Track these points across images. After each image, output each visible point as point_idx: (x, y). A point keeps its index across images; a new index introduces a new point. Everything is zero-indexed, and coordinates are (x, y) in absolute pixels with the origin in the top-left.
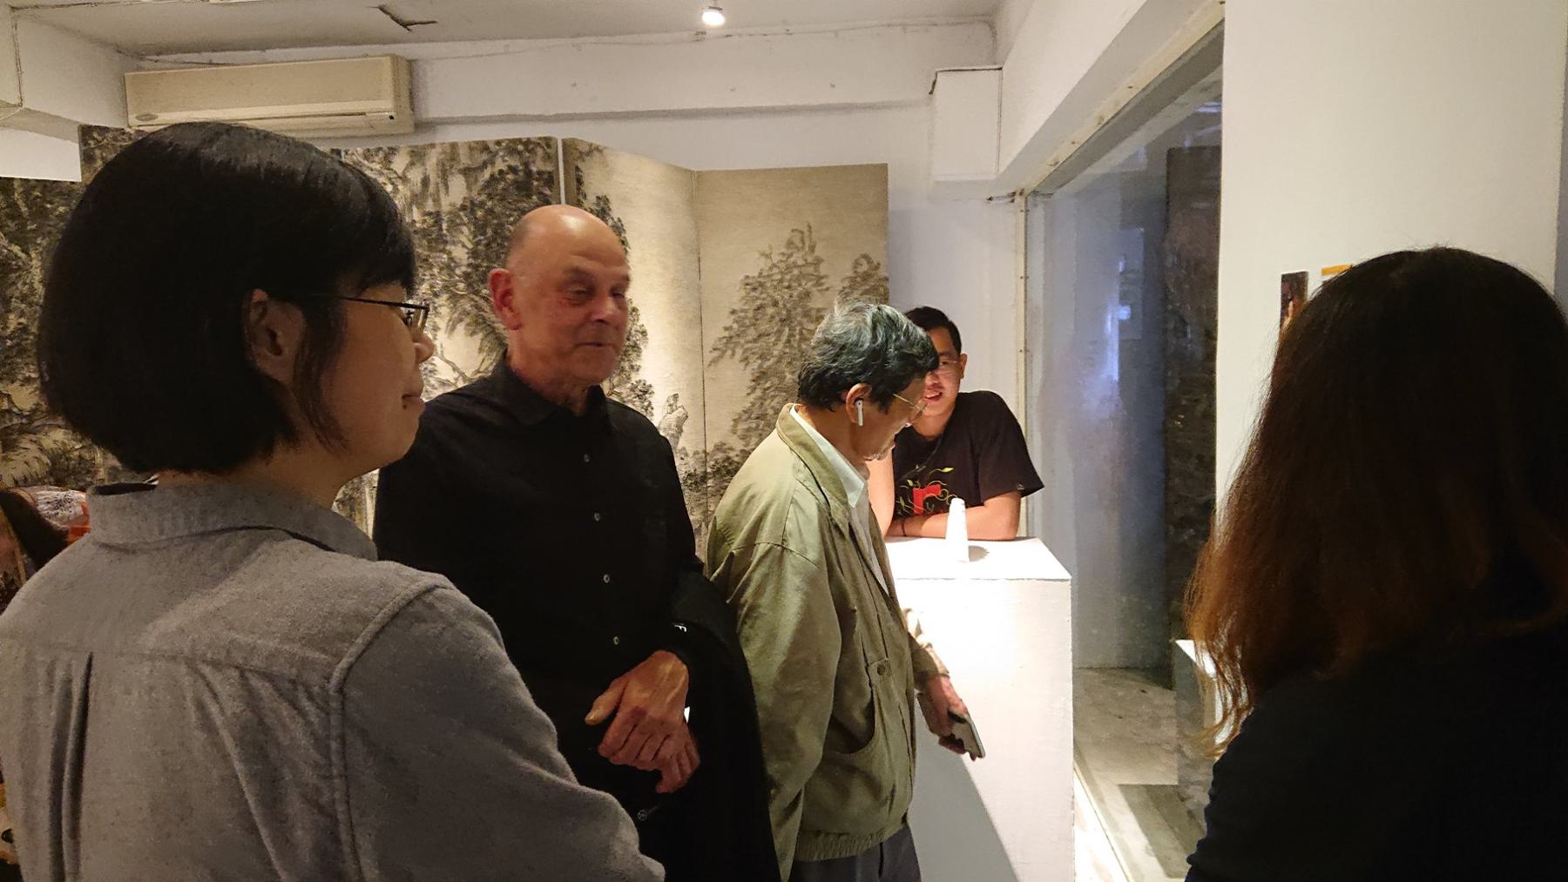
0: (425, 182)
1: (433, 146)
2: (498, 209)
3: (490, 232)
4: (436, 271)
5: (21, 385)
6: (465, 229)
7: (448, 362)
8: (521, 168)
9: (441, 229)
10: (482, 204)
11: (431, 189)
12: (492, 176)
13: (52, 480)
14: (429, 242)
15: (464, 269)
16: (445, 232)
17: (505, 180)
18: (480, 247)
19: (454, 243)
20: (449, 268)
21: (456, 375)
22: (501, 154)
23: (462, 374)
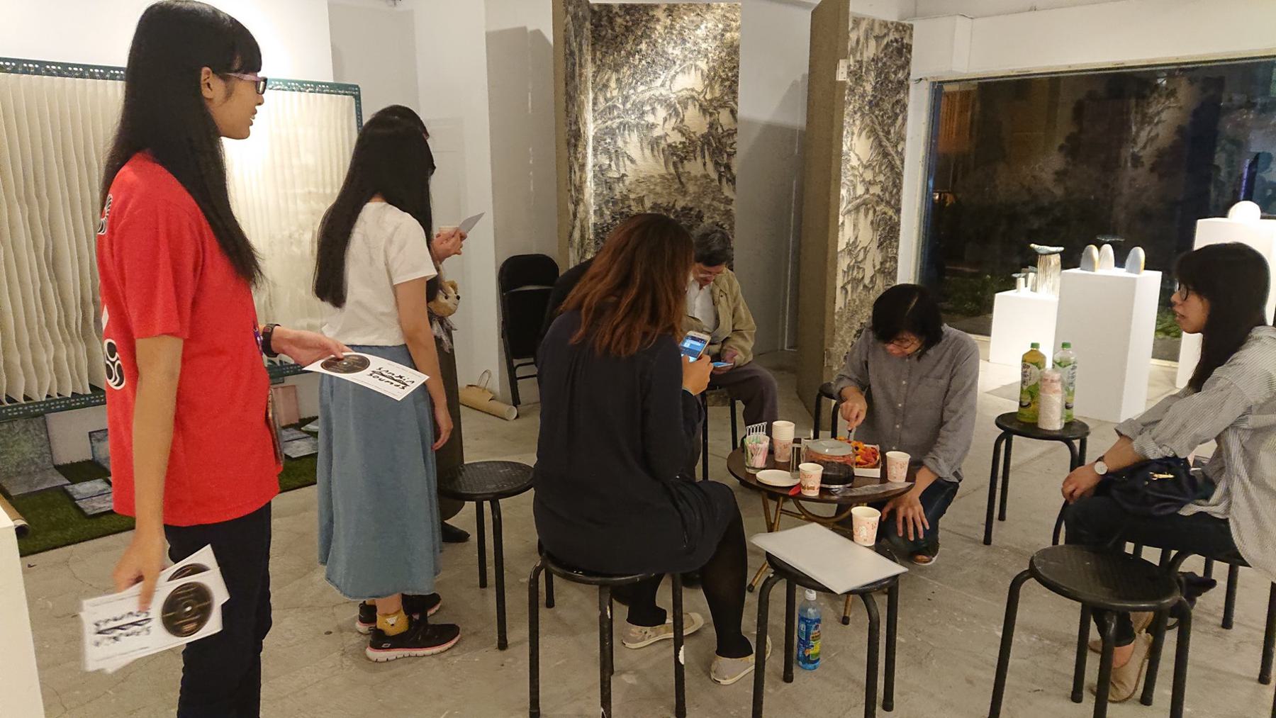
1: (864, 19)
2: (888, 63)
3: (883, 75)
4: (857, 97)
6: (872, 73)
7: (857, 155)
9: (862, 72)
10: (882, 58)
11: (860, 46)
12: (888, 42)
14: (856, 79)
15: (869, 97)
16: (863, 74)
18: (878, 85)
20: (863, 96)
21: (859, 163)
22: (893, 30)
23: (862, 162)
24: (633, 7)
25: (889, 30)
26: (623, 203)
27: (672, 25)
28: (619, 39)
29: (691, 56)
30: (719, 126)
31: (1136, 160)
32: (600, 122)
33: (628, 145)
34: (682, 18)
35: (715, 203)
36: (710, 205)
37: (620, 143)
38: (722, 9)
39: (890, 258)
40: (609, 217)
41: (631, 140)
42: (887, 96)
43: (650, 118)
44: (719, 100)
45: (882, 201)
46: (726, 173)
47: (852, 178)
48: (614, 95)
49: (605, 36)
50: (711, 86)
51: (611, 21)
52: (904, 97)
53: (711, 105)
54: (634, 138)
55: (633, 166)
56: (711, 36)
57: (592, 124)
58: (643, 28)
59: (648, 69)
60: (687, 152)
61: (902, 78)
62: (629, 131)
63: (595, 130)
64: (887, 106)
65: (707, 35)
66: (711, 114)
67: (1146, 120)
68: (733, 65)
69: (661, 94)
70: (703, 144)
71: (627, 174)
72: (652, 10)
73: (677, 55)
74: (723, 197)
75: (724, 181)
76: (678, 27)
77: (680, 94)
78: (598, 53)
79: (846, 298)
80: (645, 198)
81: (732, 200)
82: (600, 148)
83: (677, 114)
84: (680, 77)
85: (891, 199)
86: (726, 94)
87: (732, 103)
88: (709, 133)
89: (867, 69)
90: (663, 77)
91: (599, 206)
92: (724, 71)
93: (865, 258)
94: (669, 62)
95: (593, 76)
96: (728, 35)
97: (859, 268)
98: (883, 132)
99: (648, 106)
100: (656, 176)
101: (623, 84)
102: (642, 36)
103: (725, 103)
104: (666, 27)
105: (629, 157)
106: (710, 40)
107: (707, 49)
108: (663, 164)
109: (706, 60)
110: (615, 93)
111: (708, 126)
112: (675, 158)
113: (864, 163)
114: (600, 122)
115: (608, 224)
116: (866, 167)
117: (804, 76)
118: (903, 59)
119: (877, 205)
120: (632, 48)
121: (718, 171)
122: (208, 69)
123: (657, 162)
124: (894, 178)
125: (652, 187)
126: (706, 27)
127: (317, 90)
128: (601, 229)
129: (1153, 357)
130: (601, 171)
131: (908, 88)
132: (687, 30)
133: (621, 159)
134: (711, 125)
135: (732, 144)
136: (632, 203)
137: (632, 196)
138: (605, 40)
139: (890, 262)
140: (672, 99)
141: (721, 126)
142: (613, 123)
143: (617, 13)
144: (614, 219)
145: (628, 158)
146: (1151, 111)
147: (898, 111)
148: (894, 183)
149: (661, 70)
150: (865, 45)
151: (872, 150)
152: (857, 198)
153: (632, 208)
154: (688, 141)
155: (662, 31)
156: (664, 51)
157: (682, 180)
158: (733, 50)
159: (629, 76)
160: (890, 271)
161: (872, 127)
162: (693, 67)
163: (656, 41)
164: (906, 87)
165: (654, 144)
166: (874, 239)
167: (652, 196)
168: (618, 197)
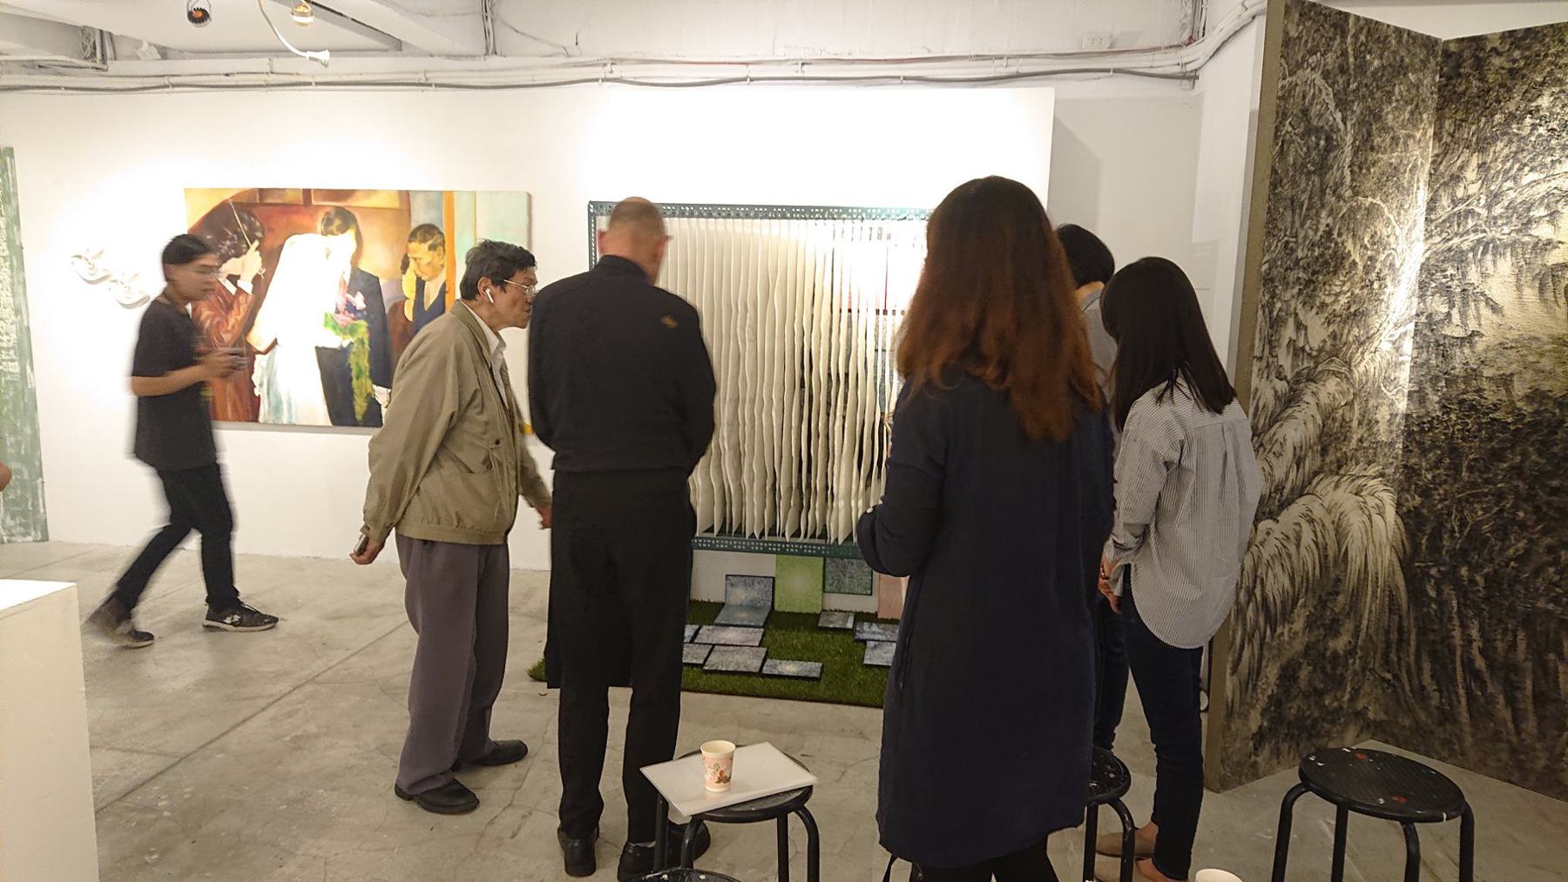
5: (1317, 313)
13: (1319, 448)
28: (1493, 94)
33: (1489, 280)
37: (1473, 275)
40: (1437, 406)
43: (1543, 231)
48: (1470, 192)
49: (1464, 93)
51: (1480, 64)
54: (1506, 266)
55: (1495, 318)
59: (1549, 141)
62: (1494, 255)
63: (1427, 255)
71: (1482, 332)
78: (1447, 123)
80: (1515, 378)
82: (1433, 285)
95: (1433, 163)
99: (1542, 209)
100: (1545, 339)
101: (1493, 172)
102: (1543, 84)
105: (1488, 300)
114: (1437, 239)
115: (1433, 418)
123: (1550, 310)
125: (1531, 359)
136: (1485, 385)
137: (1487, 372)
142: (1462, 242)
143: (1494, 49)
144: (1446, 410)
145: (1487, 304)
153: (1486, 394)
159: (1507, 156)
167: (1529, 375)
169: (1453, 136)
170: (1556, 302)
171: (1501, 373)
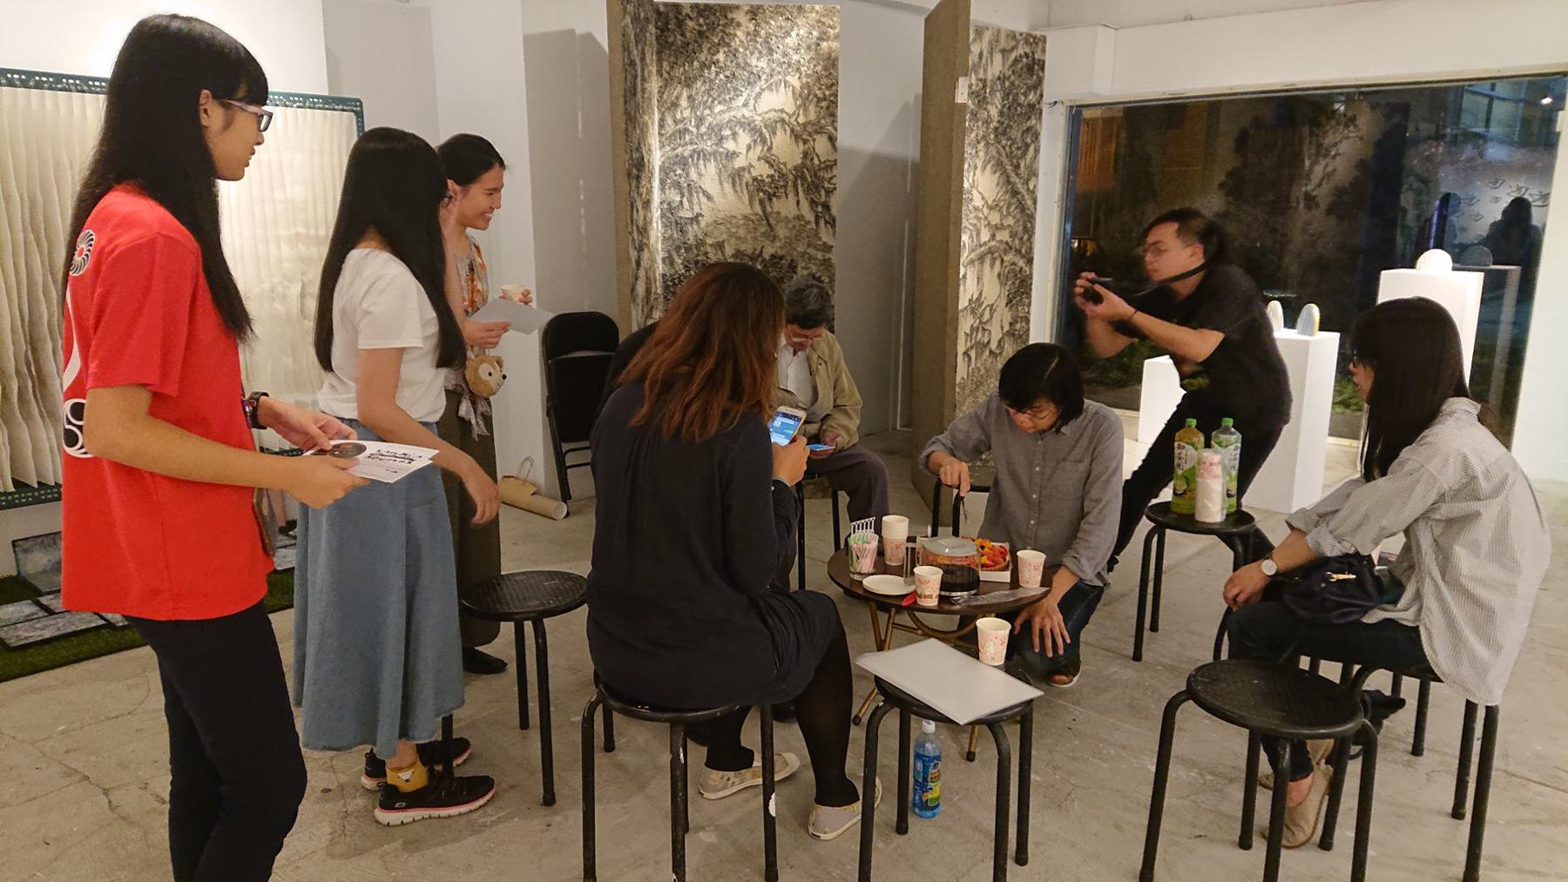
0: (981, 54)
1: (987, 28)
2: (1017, 83)
3: (1011, 97)
6: (998, 94)
7: (980, 193)
8: (1031, 54)
9: (986, 92)
10: (1010, 77)
11: (983, 61)
12: (1016, 58)
14: (979, 101)
15: (995, 124)
16: (988, 95)
17: (1022, 61)
18: (1005, 109)
19: (992, 104)
22: (1022, 42)
23: (987, 202)
24: (708, 7)
25: (1018, 42)
26: (698, 249)
27: (755, 30)
29: (780, 69)
30: (815, 156)
31: (1310, 200)
32: (668, 148)
33: (703, 178)
34: (768, 23)
35: (810, 251)
36: (805, 253)
37: (693, 175)
38: (817, 12)
39: (1021, 317)
41: (706, 171)
42: (1016, 121)
43: (730, 145)
44: (814, 125)
45: (1011, 248)
46: (824, 212)
47: (974, 221)
48: (685, 115)
49: (673, 43)
50: (804, 106)
51: (680, 24)
52: (1036, 123)
53: (805, 130)
54: (711, 169)
56: (804, 45)
57: (658, 152)
58: (720, 35)
60: (777, 188)
61: (1034, 100)
62: (704, 161)
63: (663, 159)
64: (1016, 134)
65: (799, 44)
66: (805, 142)
67: (1321, 152)
68: (831, 82)
69: (743, 115)
70: (796, 180)
71: (703, 213)
72: (731, 12)
73: (763, 68)
74: (820, 243)
75: (822, 222)
76: (763, 33)
77: (767, 116)
78: (665, 64)
79: (969, 366)
80: (726, 244)
81: (832, 247)
83: (764, 141)
84: (766, 95)
85: (1022, 247)
86: (824, 118)
87: (830, 128)
88: (803, 165)
89: (993, 91)
90: (745, 95)
91: (669, 252)
92: (820, 89)
93: (991, 317)
94: (751, 76)
95: (659, 92)
96: (824, 44)
97: (984, 330)
98: (1011, 165)
99: (728, 130)
100: (739, 217)
102: (719, 44)
103: (821, 128)
104: (748, 34)
105: (704, 192)
106: (803, 51)
107: (799, 62)
108: (747, 202)
109: (798, 75)
110: (687, 113)
111: (801, 156)
112: (761, 194)
113: (990, 202)
114: (668, 148)
116: (991, 208)
117: (917, 95)
118: (1035, 77)
119: (1005, 254)
120: (706, 59)
121: (814, 211)
122: (206, 91)
123: (740, 198)
124: (1024, 222)
125: (733, 230)
126: (798, 35)
127: (307, 104)
128: (672, 281)
129: (1330, 435)
130: (670, 210)
131: (1041, 113)
132: (774, 38)
133: (695, 194)
134: (806, 155)
135: (831, 178)
137: (709, 241)
138: (673, 48)
139: (1021, 322)
140: (757, 122)
141: (818, 156)
143: (687, 15)
146: (1326, 142)
147: (1029, 140)
148: (1025, 227)
149: (743, 86)
150: (989, 60)
151: (999, 188)
152: (981, 246)
153: (710, 255)
154: (777, 174)
155: (743, 38)
156: (746, 63)
157: (771, 222)
158: (831, 63)
159: (704, 92)
160: (1021, 333)
161: (999, 159)
162: (783, 84)
163: (737, 50)
164: (1039, 111)
165: (736, 176)
166: (1002, 296)
167: (733, 241)
168: (692, 241)
169: (669, 74)
170: (742, 192)
171: (717, 240)
